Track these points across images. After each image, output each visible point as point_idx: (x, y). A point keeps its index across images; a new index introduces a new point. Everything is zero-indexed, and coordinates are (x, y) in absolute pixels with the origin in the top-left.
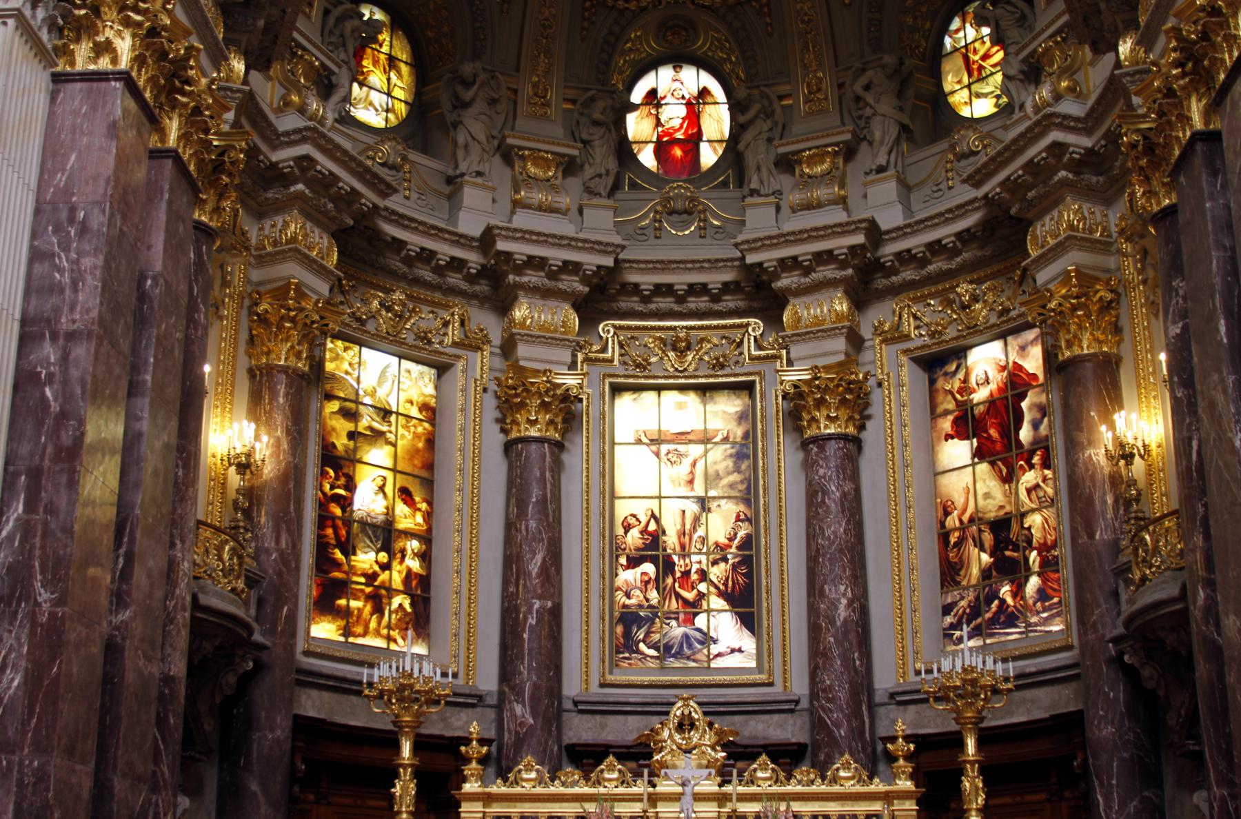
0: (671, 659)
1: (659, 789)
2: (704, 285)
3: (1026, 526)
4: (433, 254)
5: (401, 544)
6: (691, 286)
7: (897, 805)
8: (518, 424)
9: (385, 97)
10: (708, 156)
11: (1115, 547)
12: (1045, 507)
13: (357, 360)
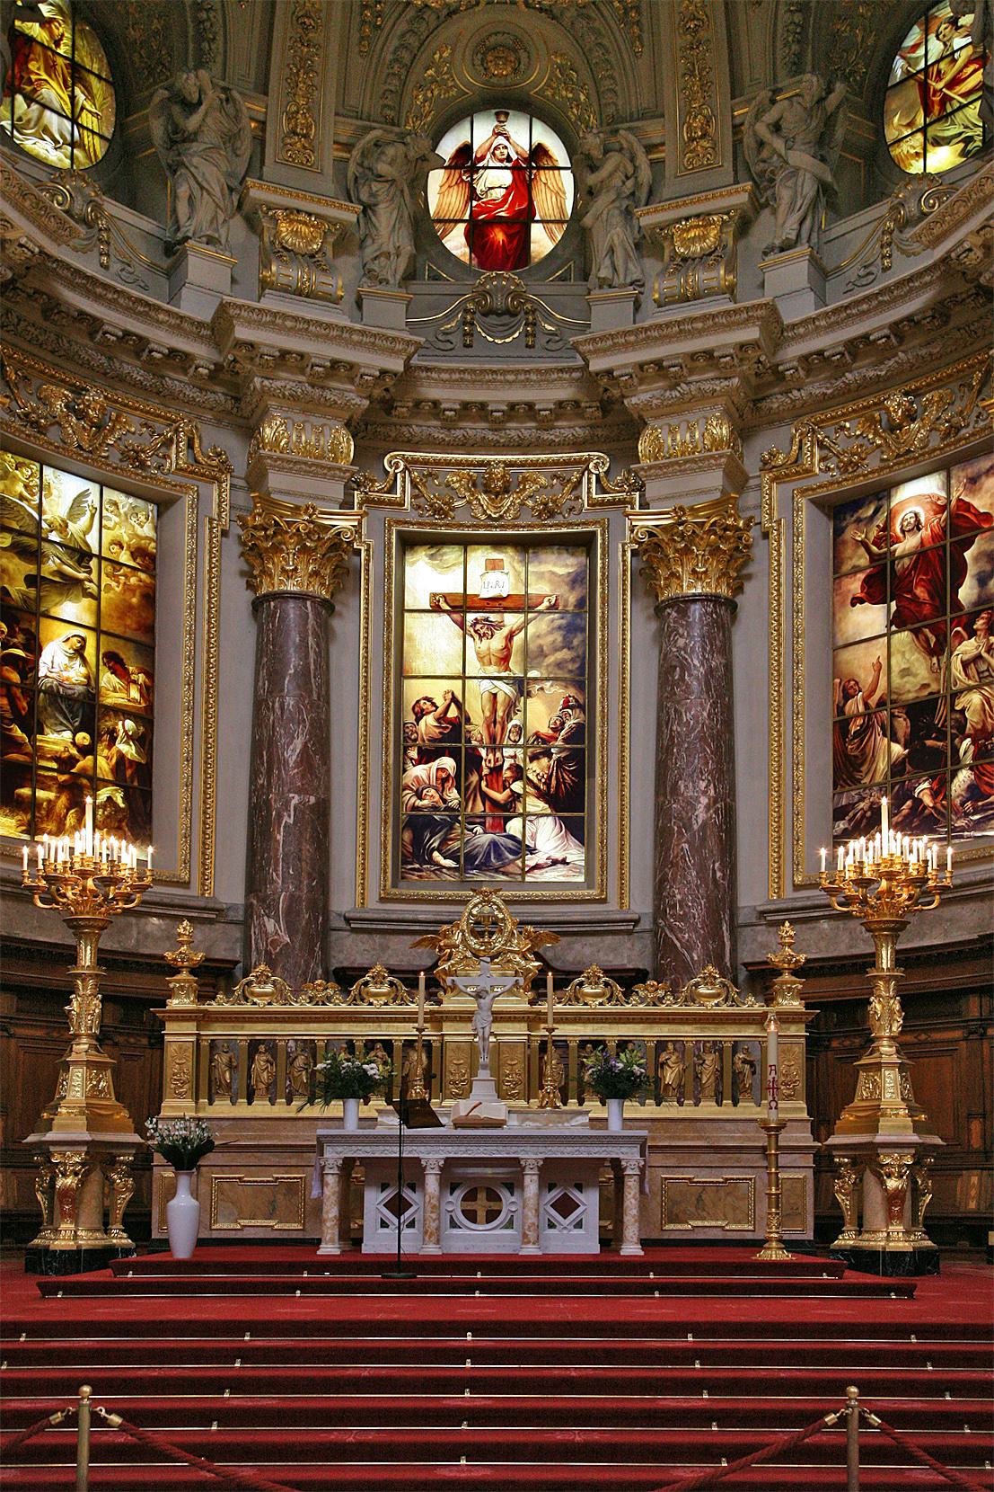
12: (987, 685)
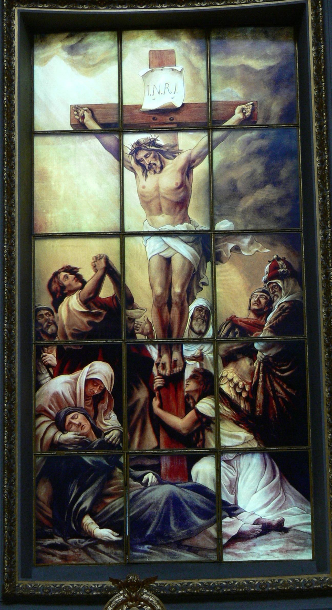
0: (146, 547)
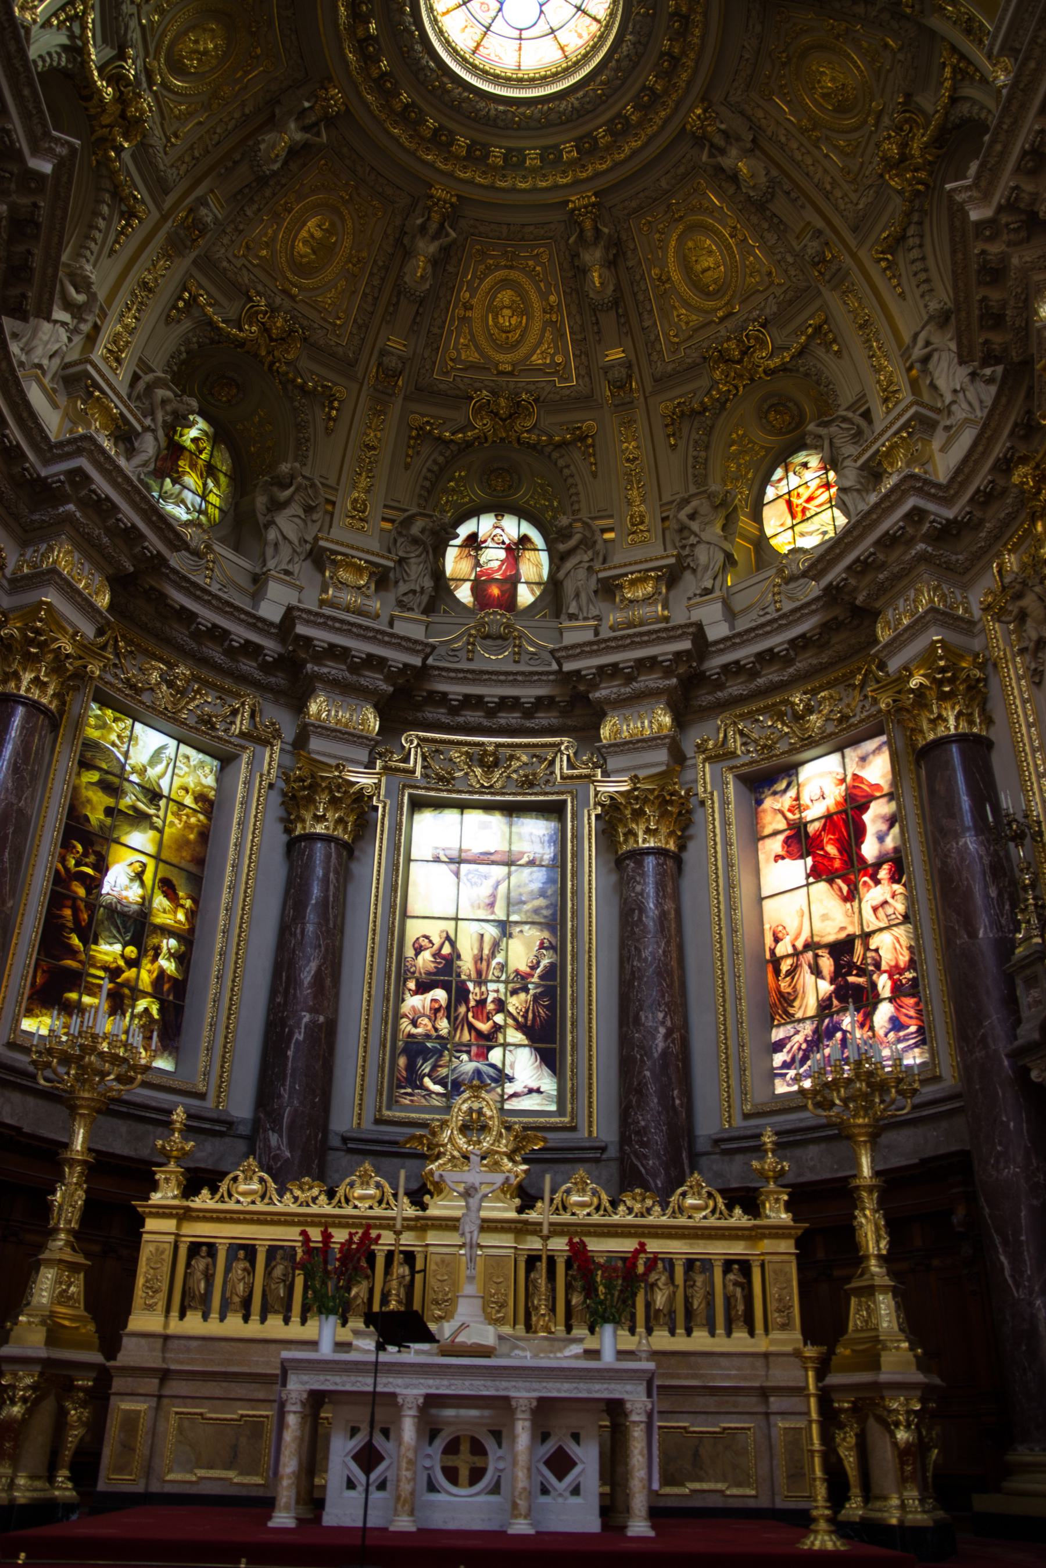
1: (432, 1212)
2: (517, 699)
3: (872, 947)
4: (226, 633)
5: (156, 941)
6: (503, 699)
7: (766, 1245)
8: (303, 821)
9: (198, 499)
10: (525, 596)
11: (1005, 946)
12: (896, 925)
13: (128, 733)
